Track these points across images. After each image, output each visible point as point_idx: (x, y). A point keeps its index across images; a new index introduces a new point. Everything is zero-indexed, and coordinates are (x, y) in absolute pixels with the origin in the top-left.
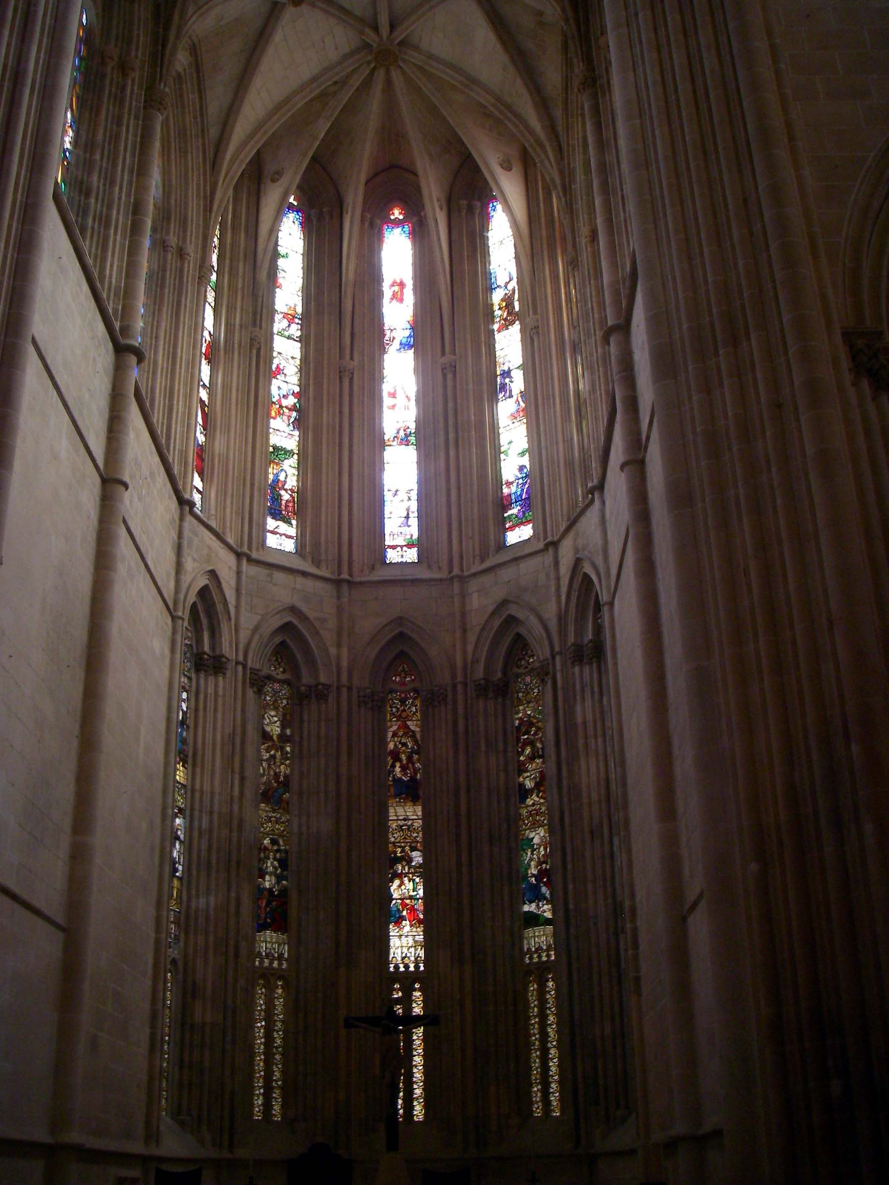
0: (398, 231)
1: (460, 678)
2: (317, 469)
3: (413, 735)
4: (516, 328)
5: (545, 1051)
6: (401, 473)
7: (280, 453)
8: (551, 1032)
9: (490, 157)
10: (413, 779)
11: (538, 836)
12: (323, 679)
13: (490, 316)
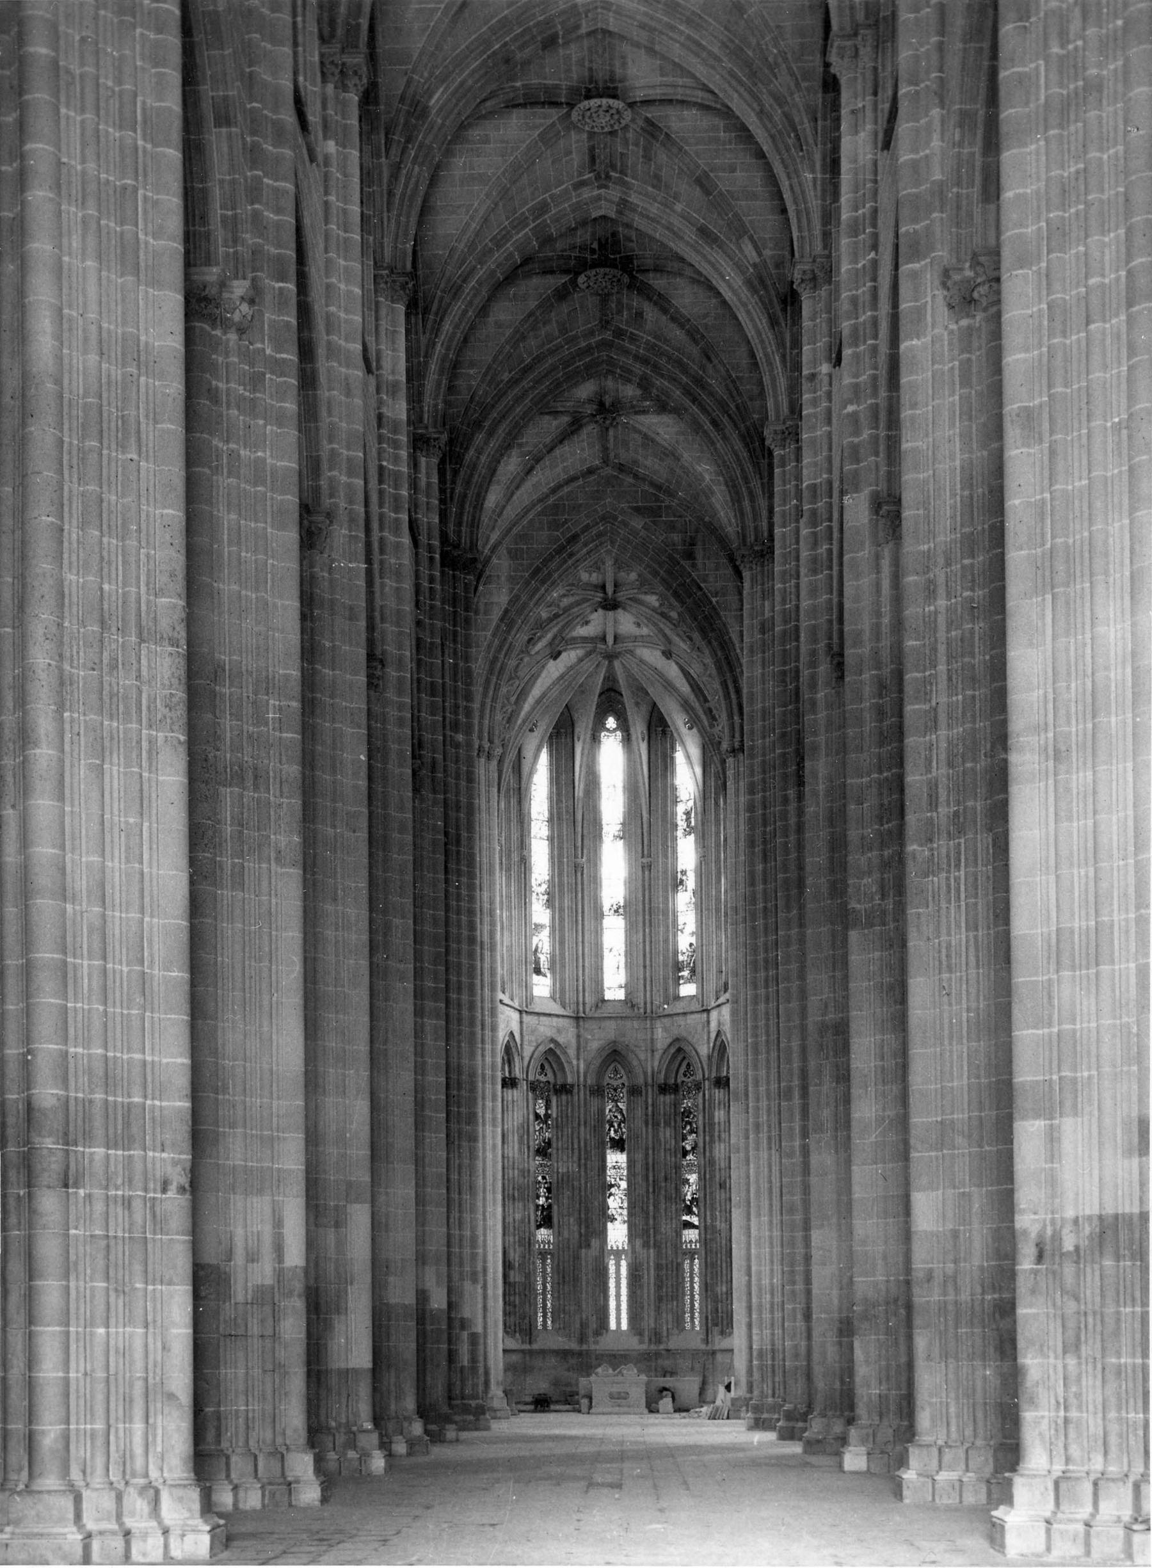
0: (612, 739)
1: (650, 1080)
2: (562, 943)
3: (621, 1112)
4: (692, 838)
5: (692, 1296)
6: (614, 934)
7: (539, 927)
8: (696, 1287)
9: (678, 720)
10: (621, 1139)
11: (693, 1178)
12: (570, 1080)
13: (675, 826)
